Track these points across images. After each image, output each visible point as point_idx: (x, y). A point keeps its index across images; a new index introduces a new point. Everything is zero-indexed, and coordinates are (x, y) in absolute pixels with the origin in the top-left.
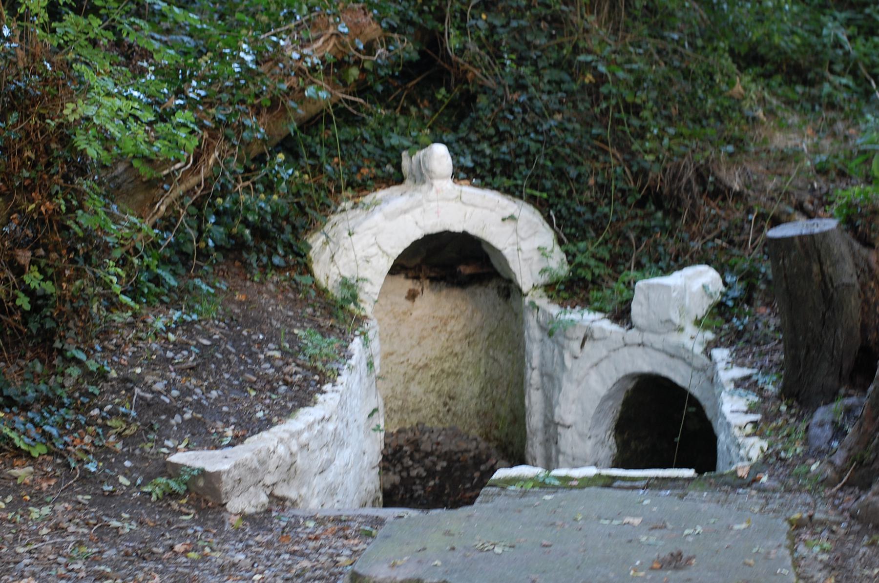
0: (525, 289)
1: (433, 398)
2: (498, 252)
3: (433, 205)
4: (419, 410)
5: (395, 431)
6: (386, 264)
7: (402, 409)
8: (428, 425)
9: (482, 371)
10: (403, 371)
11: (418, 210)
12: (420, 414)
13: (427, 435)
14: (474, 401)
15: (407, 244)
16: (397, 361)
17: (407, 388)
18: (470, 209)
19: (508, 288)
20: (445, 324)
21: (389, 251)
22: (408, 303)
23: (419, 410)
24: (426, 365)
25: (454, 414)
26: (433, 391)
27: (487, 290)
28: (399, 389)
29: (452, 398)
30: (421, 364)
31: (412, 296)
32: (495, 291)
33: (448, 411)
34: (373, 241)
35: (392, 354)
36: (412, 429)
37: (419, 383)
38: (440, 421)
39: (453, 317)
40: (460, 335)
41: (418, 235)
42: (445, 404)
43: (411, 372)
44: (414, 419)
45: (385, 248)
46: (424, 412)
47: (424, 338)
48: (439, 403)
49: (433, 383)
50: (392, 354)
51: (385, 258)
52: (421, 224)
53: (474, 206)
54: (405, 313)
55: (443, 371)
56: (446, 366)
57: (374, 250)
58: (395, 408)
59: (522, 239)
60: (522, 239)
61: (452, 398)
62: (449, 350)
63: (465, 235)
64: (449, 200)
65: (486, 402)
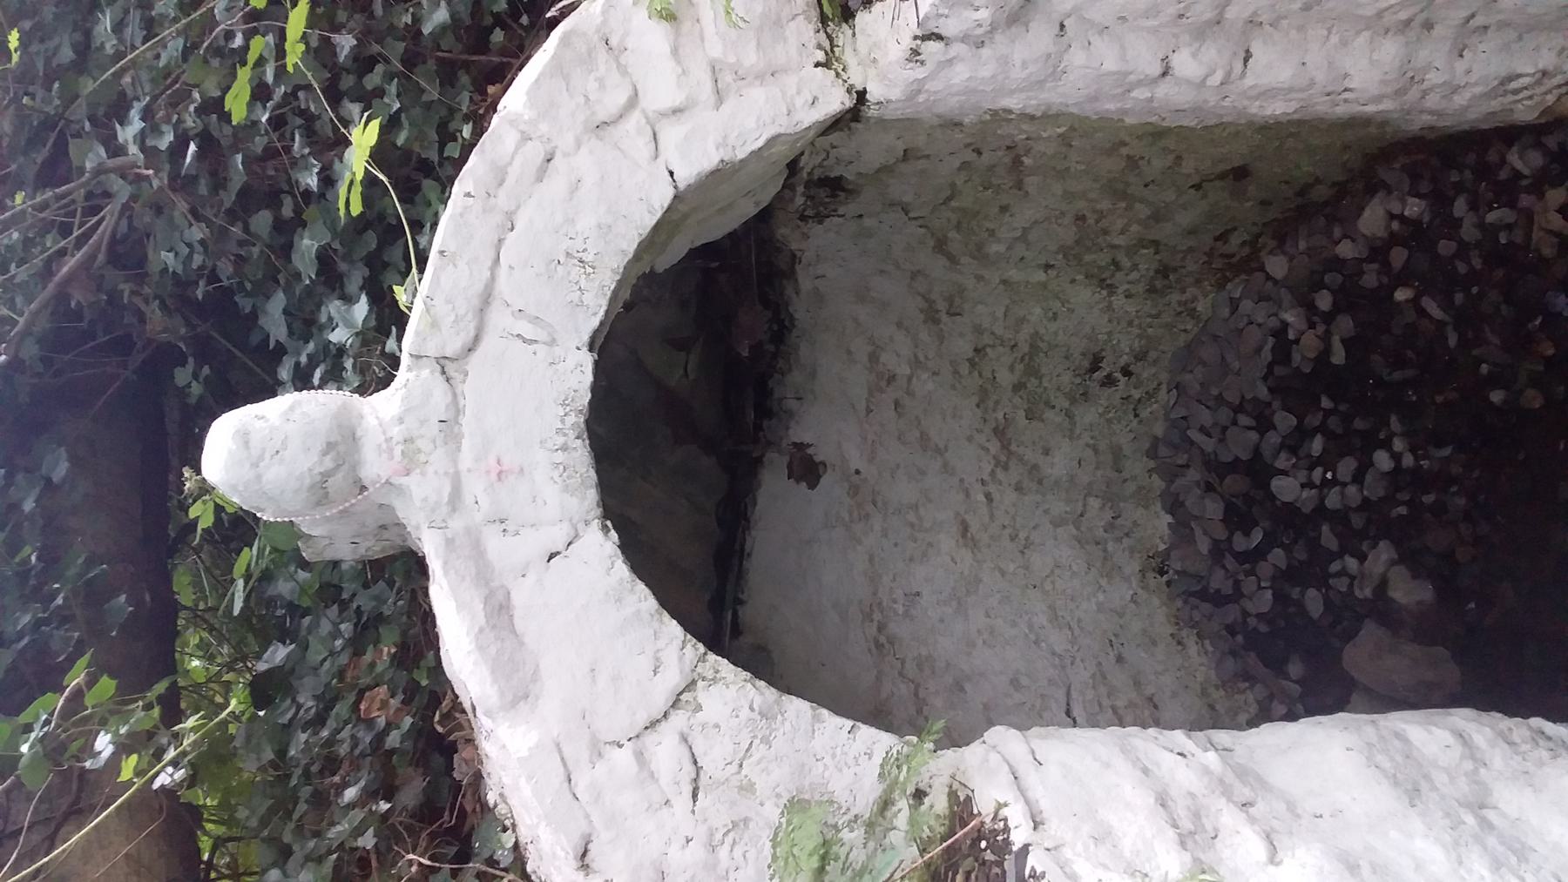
0: (836, 101)
1: (1088, 415)
2: (683, 206)
3: (474, 487)
4: (1117, 454)
5: (1169, 519)
6: (731, 692)
7: (1110, 498)
8: (1159, 429)
9: (1041, 276)
10: (1011, 496)
11: (495, 544)
12: (1127, 450)
13: (1194, 435)
14: (1118, 301)
15: (642, 599)
16: (984, 510)
17: (1057, 483)
18: (499, 320)
19: (815, 179)
20: (892, 379)
21: (671, 678)
22: (825, 481)
23: (1117, 454)
24: (999, 432)
25: (1140, 357)
26: (1069, 415)
27: (808, 256)
28: (1058, 507)
29: (1095, 367)
30: (994, 447)
31: (807, 470)
32: (816, 229)
33: (1126, 372)
34: (623, 758)
35: (965, 528)
36: (1171, 474)
37: (1046, 452)
38: (1150, 395)
39: (873, 358)
40: (924, 336)
41: (600, 550)
42: (1109, 381)
43: (1016, 473)
44: (1138, 466)
45: (660, 701)
46: (1124, 440)
47: (924, 438)
48: (1105, 396)
49: (1049, 414)
50: (965, 528)
51: (702, 694)
52: (556, 536)
53: (486, 299)
54: (854, 490)
55: (1018, 387)
56: (1006, 378)
57: (665, 749)
58: (1108, 515)
59: (633, 101)
60: (633, 101)
61: (1095, 367)
62: (964, 369)
63: (605, 345)
64: (456, 407)
65: (1135, 267)
